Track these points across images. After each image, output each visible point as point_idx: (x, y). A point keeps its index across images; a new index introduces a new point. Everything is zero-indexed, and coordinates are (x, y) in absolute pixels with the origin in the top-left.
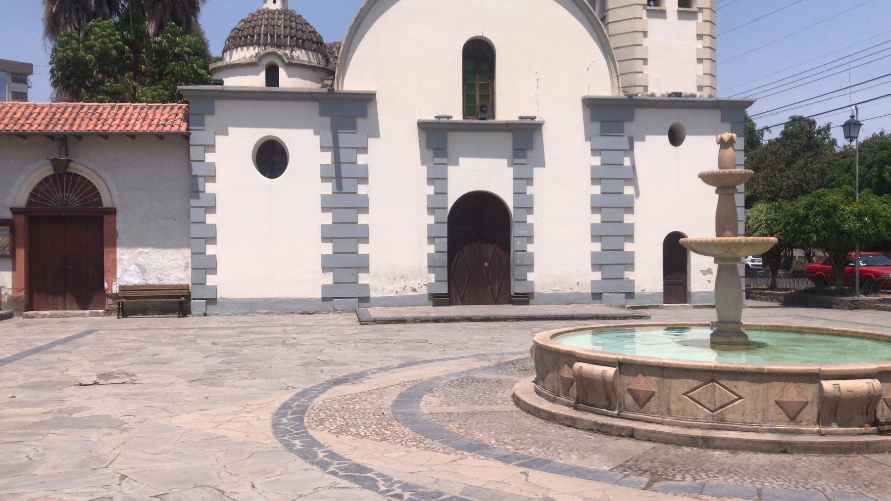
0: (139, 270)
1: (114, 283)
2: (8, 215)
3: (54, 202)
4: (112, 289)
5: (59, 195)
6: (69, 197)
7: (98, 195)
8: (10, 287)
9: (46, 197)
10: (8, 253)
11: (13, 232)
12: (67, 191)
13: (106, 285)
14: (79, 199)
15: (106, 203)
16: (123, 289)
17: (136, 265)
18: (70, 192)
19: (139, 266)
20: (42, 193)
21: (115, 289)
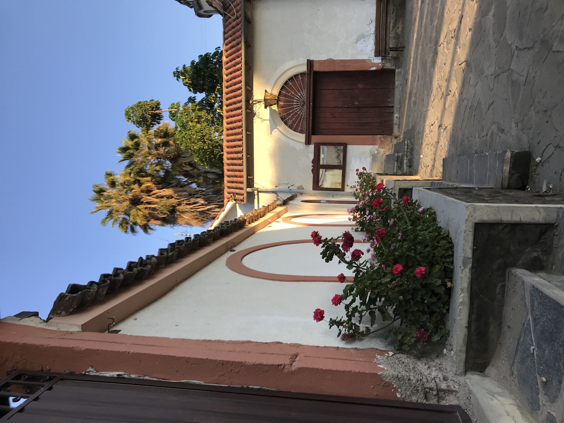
0: (362, 40)
1: (372, 62)
2: (312, 147)
3: (301, 112)
4: (378, 64)
5: (295, 107)
6: (298, 100)
7: (296, 76)
8: (371, 147)
9: (296, 119)
10: (342, 147)
11: (324, 144)
12: (293, 102)
13: (374, 68)
14: (299, 91)
15: (304, 69)
16: (378, 53)
17: (356, 43)
18: (293, 99)
19: (358, 40)
20: (294, 122)
21: (378, 60)
